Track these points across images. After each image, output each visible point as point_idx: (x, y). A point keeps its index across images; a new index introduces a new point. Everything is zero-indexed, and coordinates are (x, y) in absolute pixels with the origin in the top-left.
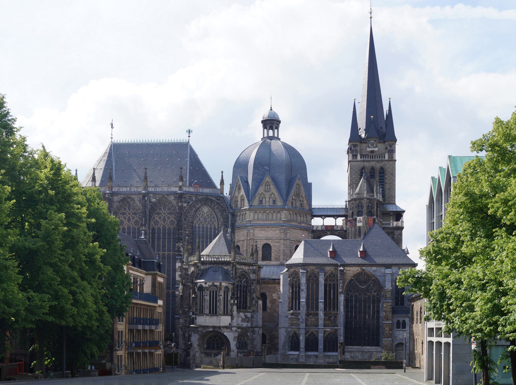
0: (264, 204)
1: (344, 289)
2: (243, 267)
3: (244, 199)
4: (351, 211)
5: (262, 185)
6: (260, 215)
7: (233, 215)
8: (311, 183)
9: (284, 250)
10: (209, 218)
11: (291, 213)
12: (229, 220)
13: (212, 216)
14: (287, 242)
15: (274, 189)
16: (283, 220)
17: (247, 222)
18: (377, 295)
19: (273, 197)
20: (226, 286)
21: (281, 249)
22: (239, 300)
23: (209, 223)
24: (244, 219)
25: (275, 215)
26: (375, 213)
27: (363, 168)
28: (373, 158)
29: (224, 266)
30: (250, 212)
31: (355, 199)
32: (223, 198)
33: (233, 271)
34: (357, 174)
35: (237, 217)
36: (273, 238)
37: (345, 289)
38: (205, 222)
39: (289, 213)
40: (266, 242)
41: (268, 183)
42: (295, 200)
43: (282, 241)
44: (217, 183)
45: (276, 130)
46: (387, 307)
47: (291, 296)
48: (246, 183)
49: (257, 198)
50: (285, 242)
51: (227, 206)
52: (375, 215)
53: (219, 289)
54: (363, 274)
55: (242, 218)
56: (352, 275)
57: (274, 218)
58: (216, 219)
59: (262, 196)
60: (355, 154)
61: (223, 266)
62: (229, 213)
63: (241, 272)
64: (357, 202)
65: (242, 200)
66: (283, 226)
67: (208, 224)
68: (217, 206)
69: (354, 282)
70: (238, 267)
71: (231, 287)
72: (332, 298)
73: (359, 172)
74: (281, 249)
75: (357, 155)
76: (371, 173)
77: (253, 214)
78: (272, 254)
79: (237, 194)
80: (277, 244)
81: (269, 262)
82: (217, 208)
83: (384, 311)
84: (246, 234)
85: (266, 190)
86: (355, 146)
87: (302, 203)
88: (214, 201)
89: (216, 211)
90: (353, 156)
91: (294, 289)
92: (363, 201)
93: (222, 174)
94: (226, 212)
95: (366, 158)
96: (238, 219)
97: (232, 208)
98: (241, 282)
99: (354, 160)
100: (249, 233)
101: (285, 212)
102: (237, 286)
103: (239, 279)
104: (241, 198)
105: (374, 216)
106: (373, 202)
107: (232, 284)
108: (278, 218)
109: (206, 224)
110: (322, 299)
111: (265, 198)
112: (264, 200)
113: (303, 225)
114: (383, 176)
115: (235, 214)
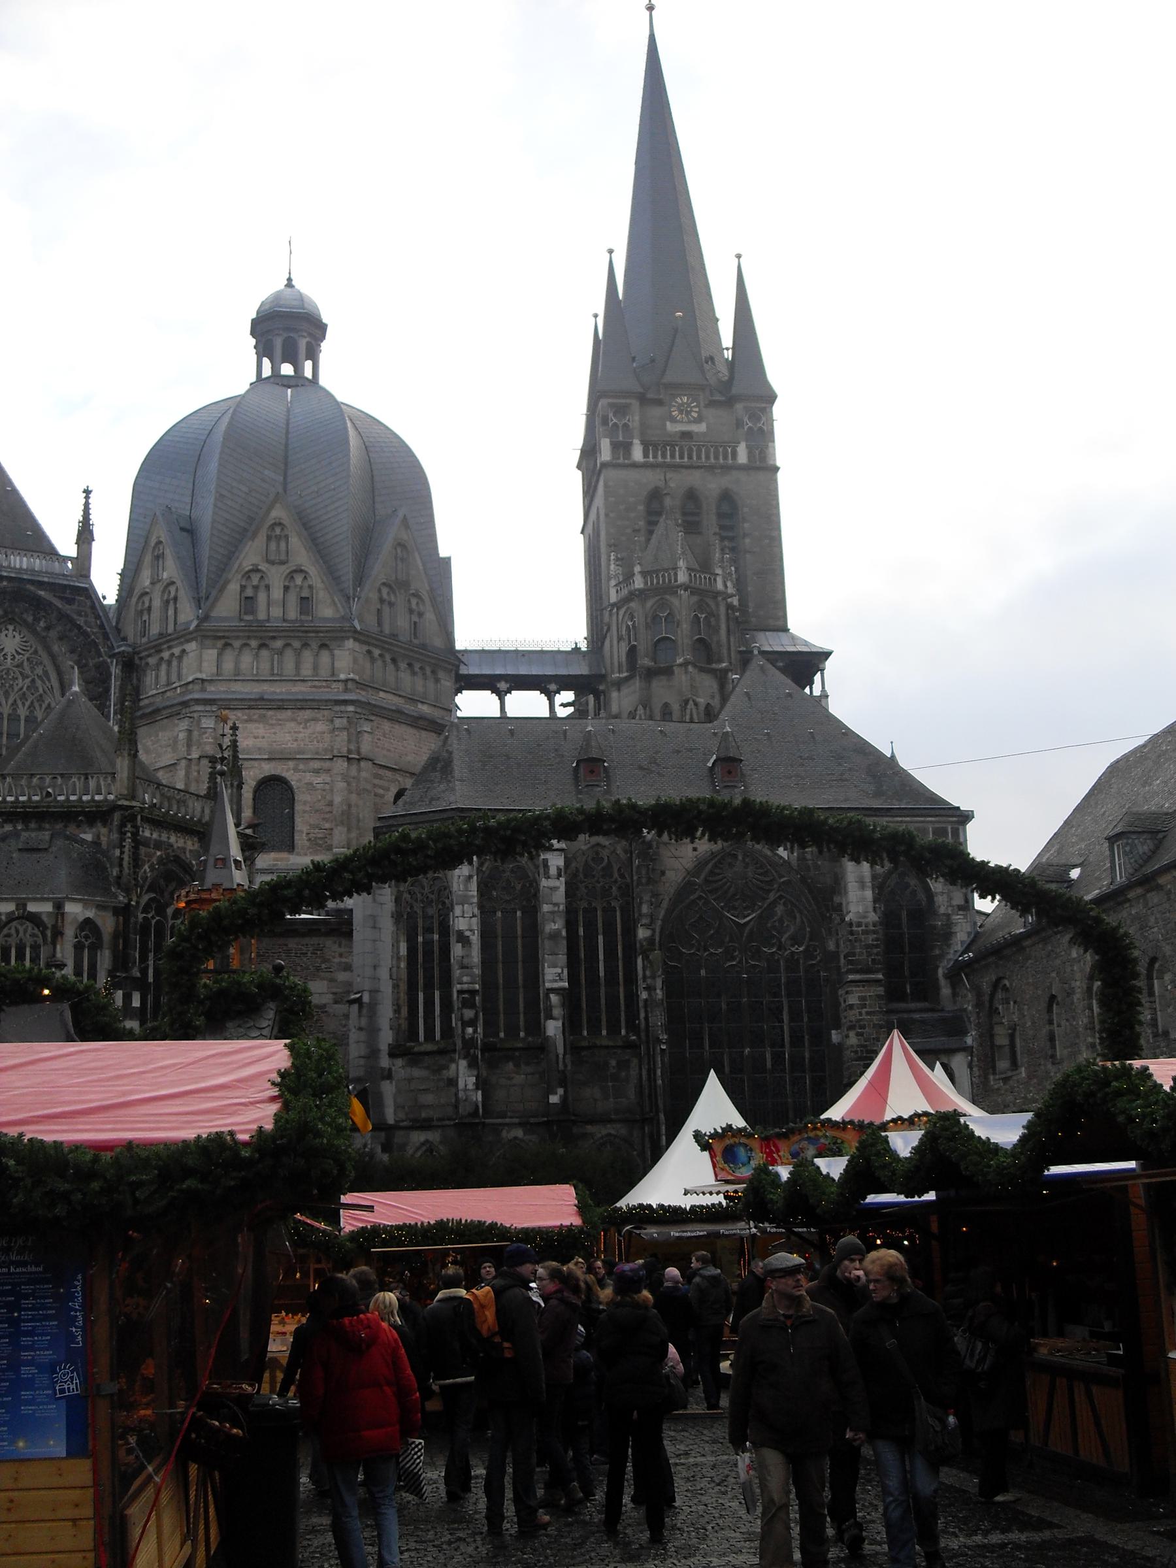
0: (262, 616)
1: (658, 930)
2: (173, 839)
3: (175, 599)
4: (624, 647)
5: (254, 536)
6: (247, 659)
7: (131, 666)
8: (449, 559)
9: (349, 806)
10: (24, 677)
11: (377, 652)
12: (108, 690)
13: (39, 671)
14: (359, 770)
15: (303, 551)
16: (342, 676)
17: (190, 687)
18: (808, 954)
19: (301, 588)
20: (88, 922)
21: (338, 799)
22: (150, 998)
23: (24, 697)
24: (174, 678)
25: (308, 656)
26: (725, 651)
27: (655, 495)
28: (690, 457)
29: (78, 826)
30: (203, 647)
31: (639, 590)
32: (88, 593)
33: (122, 847)
34: (632, 515)
35: (145, 675)
36: (299, 753)
37: (661, 933)
38: (7, 699)
39: (369, 652)
40: (268, 769)
41: (278, 531)
42: (391, 604)
43: (341, 765)
44: (66, 546)
45: (308, 365)
46: (864, 1006)
47: (404, 975)
48: (185, 534)
49: (234, 587)
50: (353, 771)
51: (102, 626)
52: (726, 659)
53: (49, 933)
54: (740, 858)
55: (168, 674)
56: (689, 866)
57: (307, 670)
58: (55, 683)
59: (255, 579)
60: (621, 439)
61: (72, 829)
62: (110, 657)
63: (160, 860)
64: (649, 604)
65: (168, 602)
66: (345, 702)
67: (19, 703)
68: (60, 628)
69: (700, 898)
70: (147, 834)
71: (107, 924)
72: (602, 974)
73: (641, 508)
74: (338, 799)
75: (631, 444)
76: (684, 514)
77: (215, 652)
78: (298, 820)
79: (147, 583)
80: (319, 780)
81: (284, 855)
82: (61, 639)
83: (851, 1028)
84: (182, 736)
85: (272, 558)
86: (621, 410)
87: (415, 618)
88: (50, 604)
89: (55, 648)
90: (615, 446)
91: (420, 939)
92: (675, 602)
93: (87, 498)
94: (100, 655)
95: (664, 456)
96: (148, 683)
97: (124, 639)
98: (161, 910)
99: (621, 461)
100: (196, 733)
101: (350, 644)
102: (145, 928)
103: (153, 895)
104: (163, 592)
105: (720, 661)
106: (713, 607)
107: (117, 911)
108: (324, 672)
109: (10, 701)
110: (561, 980)
111: (268, 587)
112: (262, 597)
113: (425, 709)
114: (731, 528)
115: (137, 661)
